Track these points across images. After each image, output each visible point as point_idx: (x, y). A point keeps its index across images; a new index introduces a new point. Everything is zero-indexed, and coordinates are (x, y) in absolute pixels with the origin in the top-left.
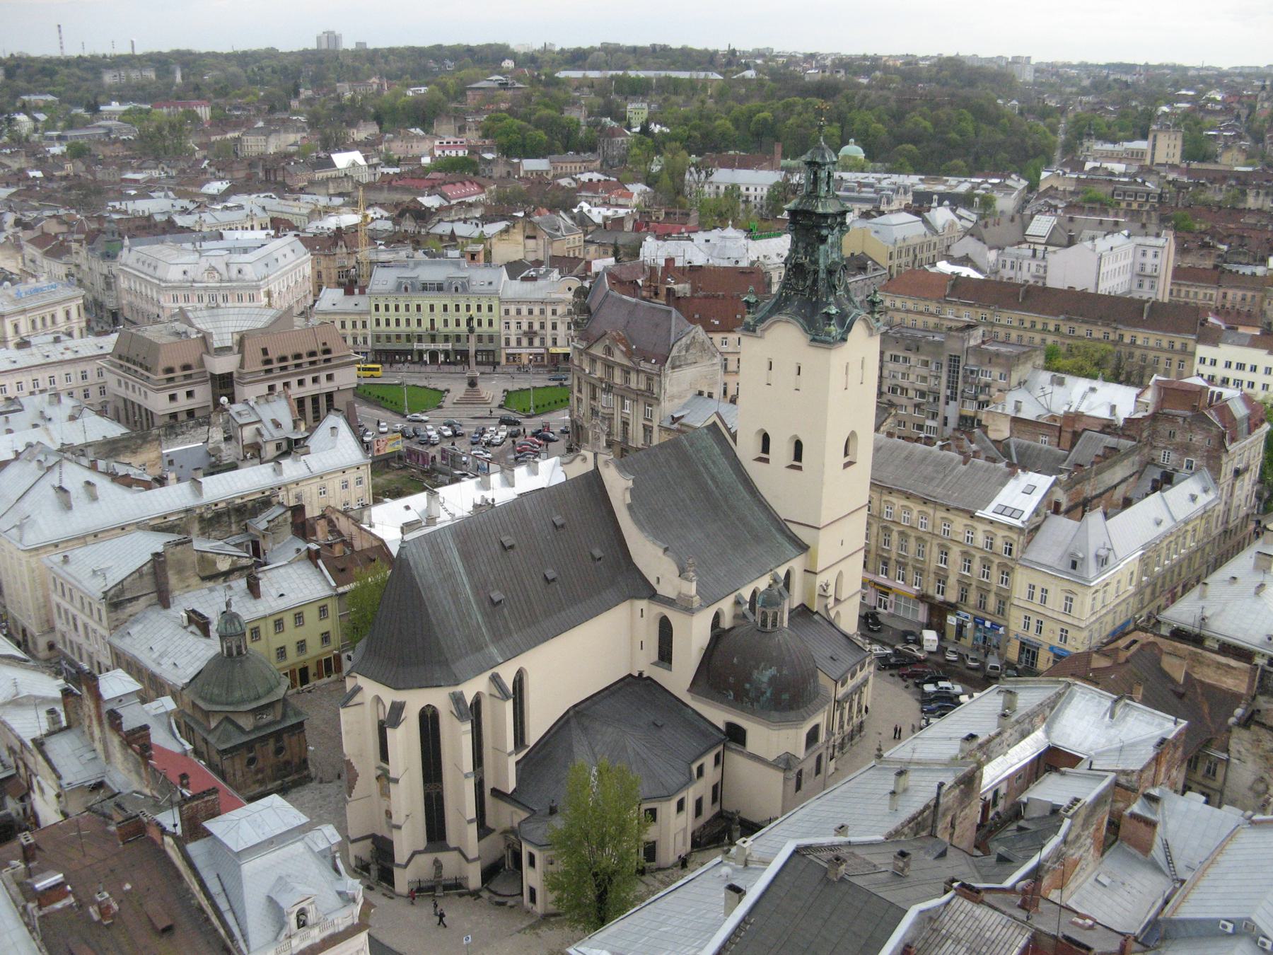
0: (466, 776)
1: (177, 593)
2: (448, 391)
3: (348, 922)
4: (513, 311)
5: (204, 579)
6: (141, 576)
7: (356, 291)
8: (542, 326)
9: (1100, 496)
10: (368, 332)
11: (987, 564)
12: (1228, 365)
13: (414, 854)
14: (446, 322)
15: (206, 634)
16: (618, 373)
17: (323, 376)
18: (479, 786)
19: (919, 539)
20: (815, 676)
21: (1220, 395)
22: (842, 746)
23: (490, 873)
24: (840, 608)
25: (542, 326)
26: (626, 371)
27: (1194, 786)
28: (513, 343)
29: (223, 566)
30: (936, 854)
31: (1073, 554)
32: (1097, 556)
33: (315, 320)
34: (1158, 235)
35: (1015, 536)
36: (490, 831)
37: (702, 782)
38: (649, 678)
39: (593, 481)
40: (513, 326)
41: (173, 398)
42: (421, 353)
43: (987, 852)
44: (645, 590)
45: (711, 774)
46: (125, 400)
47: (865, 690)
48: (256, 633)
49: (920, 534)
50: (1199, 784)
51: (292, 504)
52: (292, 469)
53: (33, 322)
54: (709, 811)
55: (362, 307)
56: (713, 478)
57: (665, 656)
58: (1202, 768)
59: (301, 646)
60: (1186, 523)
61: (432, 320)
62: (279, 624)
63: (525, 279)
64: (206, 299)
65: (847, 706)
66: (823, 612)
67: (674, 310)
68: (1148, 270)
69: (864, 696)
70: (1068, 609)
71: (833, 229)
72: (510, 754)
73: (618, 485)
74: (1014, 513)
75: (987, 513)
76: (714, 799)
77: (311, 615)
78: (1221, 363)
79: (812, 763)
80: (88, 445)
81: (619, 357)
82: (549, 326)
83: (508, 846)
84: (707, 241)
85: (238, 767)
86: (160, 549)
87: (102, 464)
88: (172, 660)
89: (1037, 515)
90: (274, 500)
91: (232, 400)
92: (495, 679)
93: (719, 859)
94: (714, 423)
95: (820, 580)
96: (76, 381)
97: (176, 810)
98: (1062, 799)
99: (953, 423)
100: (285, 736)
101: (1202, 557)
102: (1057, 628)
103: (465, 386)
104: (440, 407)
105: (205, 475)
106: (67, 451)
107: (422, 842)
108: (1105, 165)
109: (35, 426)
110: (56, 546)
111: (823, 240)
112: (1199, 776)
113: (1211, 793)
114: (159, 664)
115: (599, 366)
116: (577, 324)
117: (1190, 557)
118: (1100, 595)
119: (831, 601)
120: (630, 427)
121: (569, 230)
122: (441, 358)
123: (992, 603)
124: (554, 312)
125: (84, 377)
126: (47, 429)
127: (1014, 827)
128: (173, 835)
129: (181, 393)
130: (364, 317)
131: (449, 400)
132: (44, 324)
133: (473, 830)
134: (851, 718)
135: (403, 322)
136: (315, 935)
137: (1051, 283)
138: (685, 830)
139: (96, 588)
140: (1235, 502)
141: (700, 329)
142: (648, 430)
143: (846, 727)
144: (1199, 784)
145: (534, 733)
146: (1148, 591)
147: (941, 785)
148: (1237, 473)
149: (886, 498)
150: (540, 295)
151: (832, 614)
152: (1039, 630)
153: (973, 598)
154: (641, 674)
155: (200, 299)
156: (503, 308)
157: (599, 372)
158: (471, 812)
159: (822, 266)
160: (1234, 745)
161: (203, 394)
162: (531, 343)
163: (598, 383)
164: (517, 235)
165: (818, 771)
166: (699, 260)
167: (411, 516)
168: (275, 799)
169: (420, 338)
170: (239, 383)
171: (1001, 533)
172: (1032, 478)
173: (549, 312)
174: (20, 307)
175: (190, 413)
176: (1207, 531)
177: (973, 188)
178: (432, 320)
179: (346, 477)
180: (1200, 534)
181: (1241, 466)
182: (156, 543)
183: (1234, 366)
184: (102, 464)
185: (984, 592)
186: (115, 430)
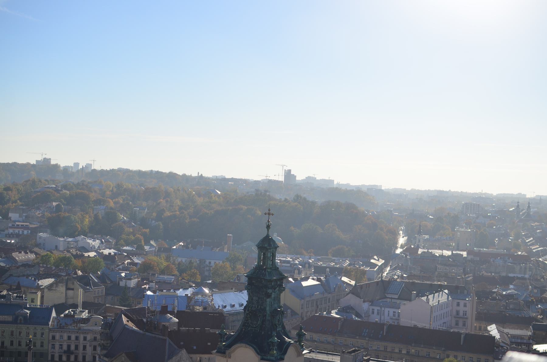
8: (77, 347)
14: (12, 343)
25: (77, 347)
67: (167, 339)
68: (461, 314)
71: (275, 289)
82: (81, 348)
108: (430, 251)
111: (269, 296)
116: (103, 347)
121: (95, 285)
124: (85, 339)
137: (402, 324)
141: (184, 352)
159: (268, 312)
164: (62, 289)
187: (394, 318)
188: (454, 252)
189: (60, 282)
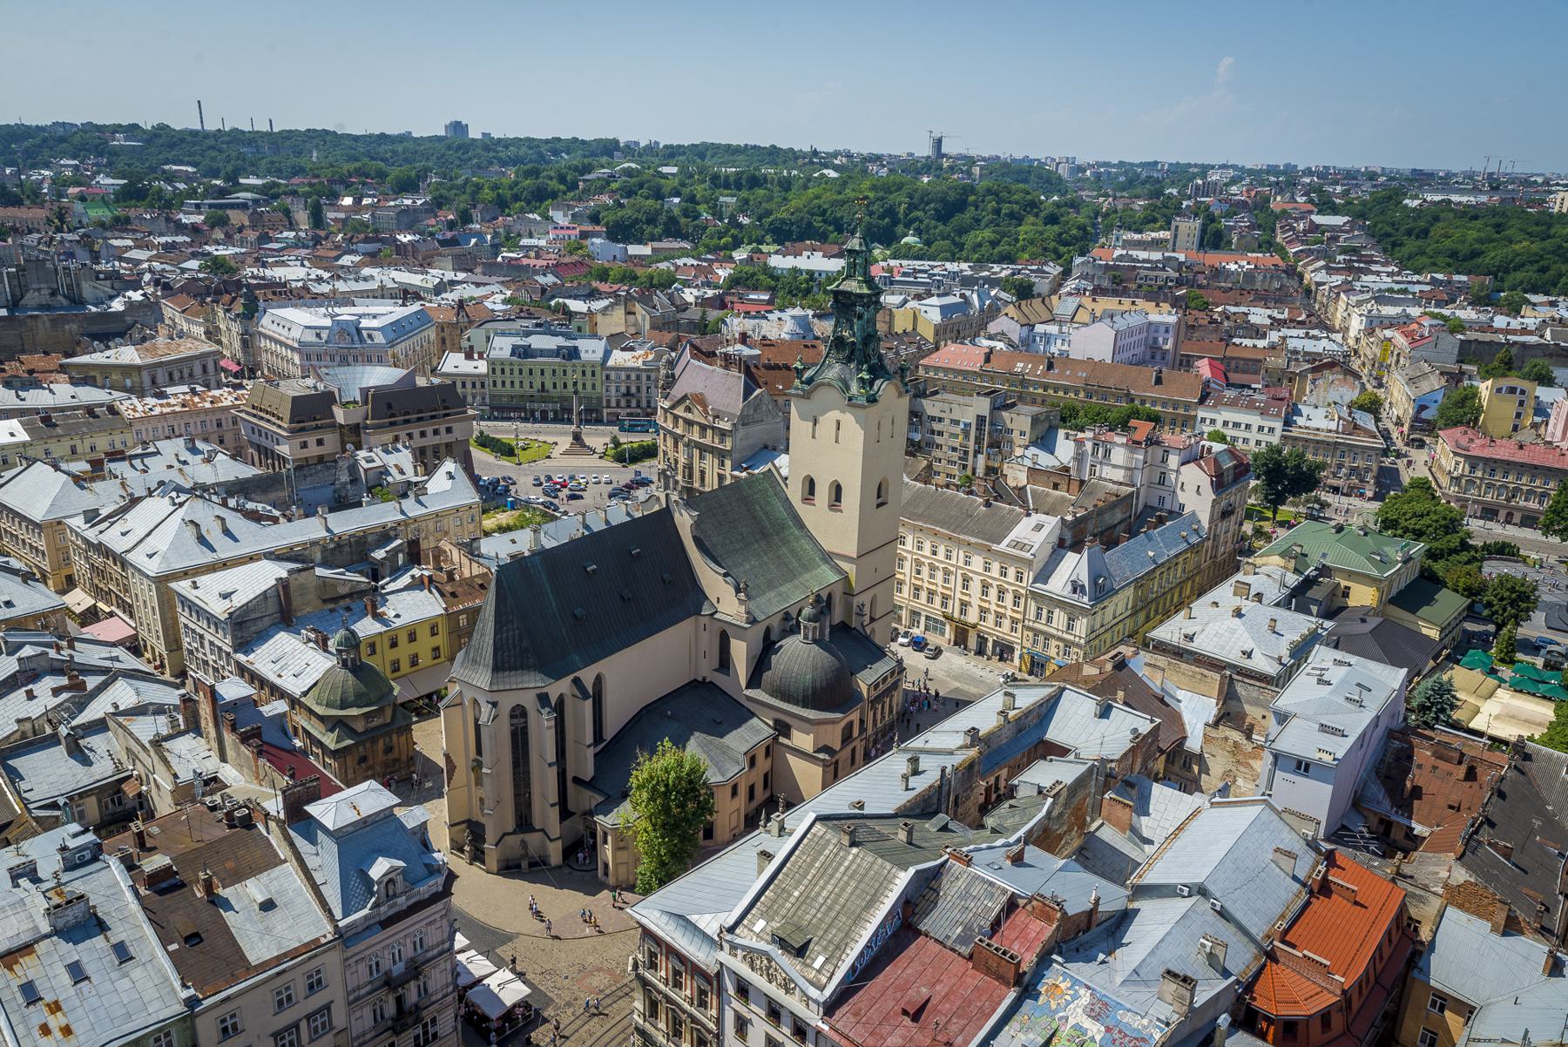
0: (550, 765)
3: (434, 890)
4: (613, 375)
5: (325, 601)
7: (476, 356)
8: (638, 389)
9: (1102, 533)
10: (487, 391)
12: (1226, 423)
13: (505, 834)
14: (555, 385)
16: (696, 428)
17: (443, 429)
18: (562, 776)
21: (1210, 449)
22: (875, 741)
23: (569, 852)
24: (875, 625)
25: (638, 389)
26: (703, 428)
27: (1173, 777)
28: (613, 404)
29: (343, 590)
31: (1074, 582)
32: (1096, 584)
33: (436, 381)
34: (1170, 313)
37: (754, 770)
38: (711, 682)
41: (304, 445)
43: (982, 826)
48: (372, 646)
51: (410, 536)
52: (411, 508)
54: (761, 795)
56: (766, 513)
57: (725, 664)
59: (414, 661)
60: (1177, 556)
61: (543, 384)
63: (623, 350)
73: (684, 521)
75: (1002, 547)
76: (765, 787)
80: (219, 484)
85: (349, 764)
86: (284, 575)
90: (392, 533)
91: (359, 447)
92: (577, 681)
95: (856, 601)
97: (280, 798)
98: (1047, 784)
99: (980, 471)
100: (395, 737)
101: (1192, 587)
103: (570, 439)
104: (549, 457)
105: (331, 510)
106: (200, 491)
107: (510, 825)
108: (1130, 252)
109: (170, 467)
110: (186, 573)
112: (1176, 768)
114: (280, 676)
115: (681, 421)
117: (1181, 584)
119: (867, 619)
124: (649, 378)
125: (219, 425)
126: (180, 470)
127: (1006, 805)
128: (278, 821)
130: (482, 379)
131: (556, 452)
133: (554, 813)
134: (883, 718)
135: (517, 384)
136: (402, 902)
138: (738, 810)
139: (219, 609)
142: (721, 477)
143: (879, 725)
145: (611, 730)
146: (1141, 616)
147: (943, 770)
148: (1226, 514)
150: (640, 364)
154: (704, 679)
155: (332, 360)
156: (604, 373)
161: (331, 441)
162: (628, 401)
164: (619, 313)
165: (853, 762)
167: (514, 549)
169: (531, 398)
170: (369, 434)
173: (644, 378)
174: (156, 360)
175: (321, 459)
176: (1198, 566)
177: (1013, 274)
178: (543, 384)
180: (1190, 566)
182: (280, 570)
183: (1231, 425)
184: (232, 502)
186: (246, 471)
187: (1064, 348)
188: (1167, 254)
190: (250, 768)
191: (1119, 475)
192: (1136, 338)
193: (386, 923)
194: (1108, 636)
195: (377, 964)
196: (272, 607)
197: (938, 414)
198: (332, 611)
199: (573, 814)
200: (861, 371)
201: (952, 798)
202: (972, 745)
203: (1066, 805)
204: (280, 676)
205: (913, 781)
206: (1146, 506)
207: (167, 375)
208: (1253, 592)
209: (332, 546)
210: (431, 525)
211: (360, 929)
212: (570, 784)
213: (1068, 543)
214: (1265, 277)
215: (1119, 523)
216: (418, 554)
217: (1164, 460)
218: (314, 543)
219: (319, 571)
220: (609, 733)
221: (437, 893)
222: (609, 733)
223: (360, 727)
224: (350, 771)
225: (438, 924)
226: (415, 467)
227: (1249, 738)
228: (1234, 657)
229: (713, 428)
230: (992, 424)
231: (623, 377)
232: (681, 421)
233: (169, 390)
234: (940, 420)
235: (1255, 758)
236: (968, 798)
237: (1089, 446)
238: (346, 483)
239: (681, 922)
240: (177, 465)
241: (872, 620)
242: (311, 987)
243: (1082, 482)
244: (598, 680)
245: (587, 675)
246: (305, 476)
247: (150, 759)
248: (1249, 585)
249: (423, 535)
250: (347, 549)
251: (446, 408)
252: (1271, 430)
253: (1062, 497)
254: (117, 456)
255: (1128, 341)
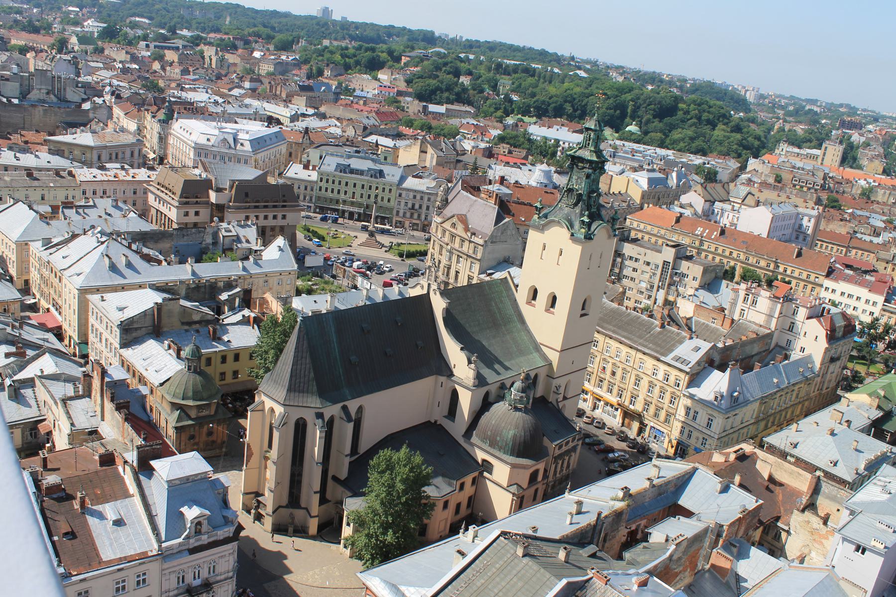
1: (165, 329)
2: (356, 237)
3: (226, 535)
4: (404, 193)
5: (183, 323)
6: (145, 315)
7: (311, 168)
8: (420, 207)
9: (742, 360)
10: (314, 193)
11: (663, 391)
12: (843, 294)
13: (280, 507)
15: (179, 356)
16: (458, 240)
17: (280, 215)
19: (624, 369)
20: (541, 441)
21: (829, 311)
22: (553, 487)
24: (565, 402)
25: (420, 207)
26: (463, 240)
27: (765, 544)
28: (401, 214)
29: (196, 318)
30: (590, 554)
33: (281, 181)
34: (813, 208)
35: (682, 375)
36: (328, 501)
37: (462, 492)
39: (424, 301)
40: (403, 204)
41: (187, 214)
42: (344, 212)
44: (445, 370)
45: (469, 490)
46: (157, 210)
47: (573, 454)
49: (625, 366)
50: (769, 543)
51: (246, 287)
53: (111, 154)
54: (464, 511)
55: (309, 179)
58: (772, 534)
59: (235, 373)
62: (224, 359)
63: (413, 176)
64: (218, 158)
65: (560, 462)
66: (555, 403)
69: (572, 458)
70: (709, 425)
71: (595, 170)
72: (347, 456)
73: (439, 304)
74: (684, 362)
75: (668, 359)
77: (244, 357)
78: (838, 293)
79: (532, 490)
80: (128, 233)
81: (460, 230)
82: (424, 207)
83: (337, 512)
84: (530, 170)
85: (183, 438)
86: (160, 301)
87: (134, 247)
88: (155, 369)
89: (699, 365)
90: (234, 283)
91: (222, 220)
92: (345, 408)
93: (457, 536)
94: (506, 278)
95: (555, 383)
96: (129, 194)
97: (135, 453)
98: (672, 536)
99: (660, 301)
101: (802, 409)
102: (701, 436)
104: (351, 246)
106: (115, 235)
107: (285, 501)
113: (776, 550)
114: (147, 370)
118: (730, 420)
119: (561, 397)
120: (460, 275)
122: (356, 216)
123: (663, 415)
124: (429, 200)
128: (132, 466)
129: (192, 212)
132: (117, 157)
133: (316, 498)
134: (562, 470)
136: (205, 539)
138: (446, 519)
140: (828, 376)
142: (470, 278)
143: (558, 475)
144: (769, 543)
146: (762, 425)
147: (599, 514)
148: (833, 360)
149: (608, 340)
150: (424, 188)
151: (561, 405)
152: (690, 436)
153: (652, 409)
154: (436, 422)
155: (215, 157)
157: (447, 239)
158: (317, 486)
160: (792, 523)
161: (205, 213)
162: (412, 214)
163: (445, 246)
164: (416, 149)
165: (534, 499)
166: (523, 182)
167: (316, 307)
168: (194, 454)
169: (344, 202)
170: (228, 211)
171: (674, 373)
172: (697, 342)
175: (195, 225)
176: (808, 394)
177: (704, 164)
179: (281, 277)
180: (802, 394)
181: (835, 356)
182: (158, 297)
183: (846, 295)
184: (134, 247)
185: (658, 409)
189: (415, 144)
190: (119, 428)
191: (761, 319)
192: (787, 222)
193: (193, 551)
194: (735, 436)
195: (183, 577)
196: (148, 322)
197: (635, 256)
198: (187, 331)
199: (330, 501)
200: (583, 215)
201: (602, 535)
202: (623, 500)
203: (684, 553)
204: (147, 370)
205: (577, 518)
206: (777, 345)
207: (108, 155)
208: (845, 419)
209: (193, 286)
210: (261, 281)
211: (175, 551)
212: (330, 482)
213: (716, 364)
214: (885, 193)
215: (756, 355)
216: (249, 301)
217: (795, 313)
218: (182, 282)
219: (183, 302)
220: (364, 447)
221: (229, 537)
222: (364, 447)
223: (193, 414)
224: (183, 444)
225: (227, 559)
226: (257, 239)
227: (825, 523)
228: (822, 462)
229: (470, 242)
230: (673, 268)
231: (411, 197)
232: (447, 233)
233: (108, 165)
234: (636, 260)
235: (827, 538)
236: (614, 537)
237: (742, 294)
238: (210, 244)
239: (393, 589)
240: (104, 216)
241: (565, 398)
242: (138, 583)
243: (733, 321)
244: (360, 409)
245: (353, 405)
246: (184, 236)
247: (59, 411)
248: (843, 414)
249: (254, 288)
250: (203, 290)
251: (285, 201)
252: (875, 303)
253: (717, 330)
254: (68, 205)
255: (780, 223)
